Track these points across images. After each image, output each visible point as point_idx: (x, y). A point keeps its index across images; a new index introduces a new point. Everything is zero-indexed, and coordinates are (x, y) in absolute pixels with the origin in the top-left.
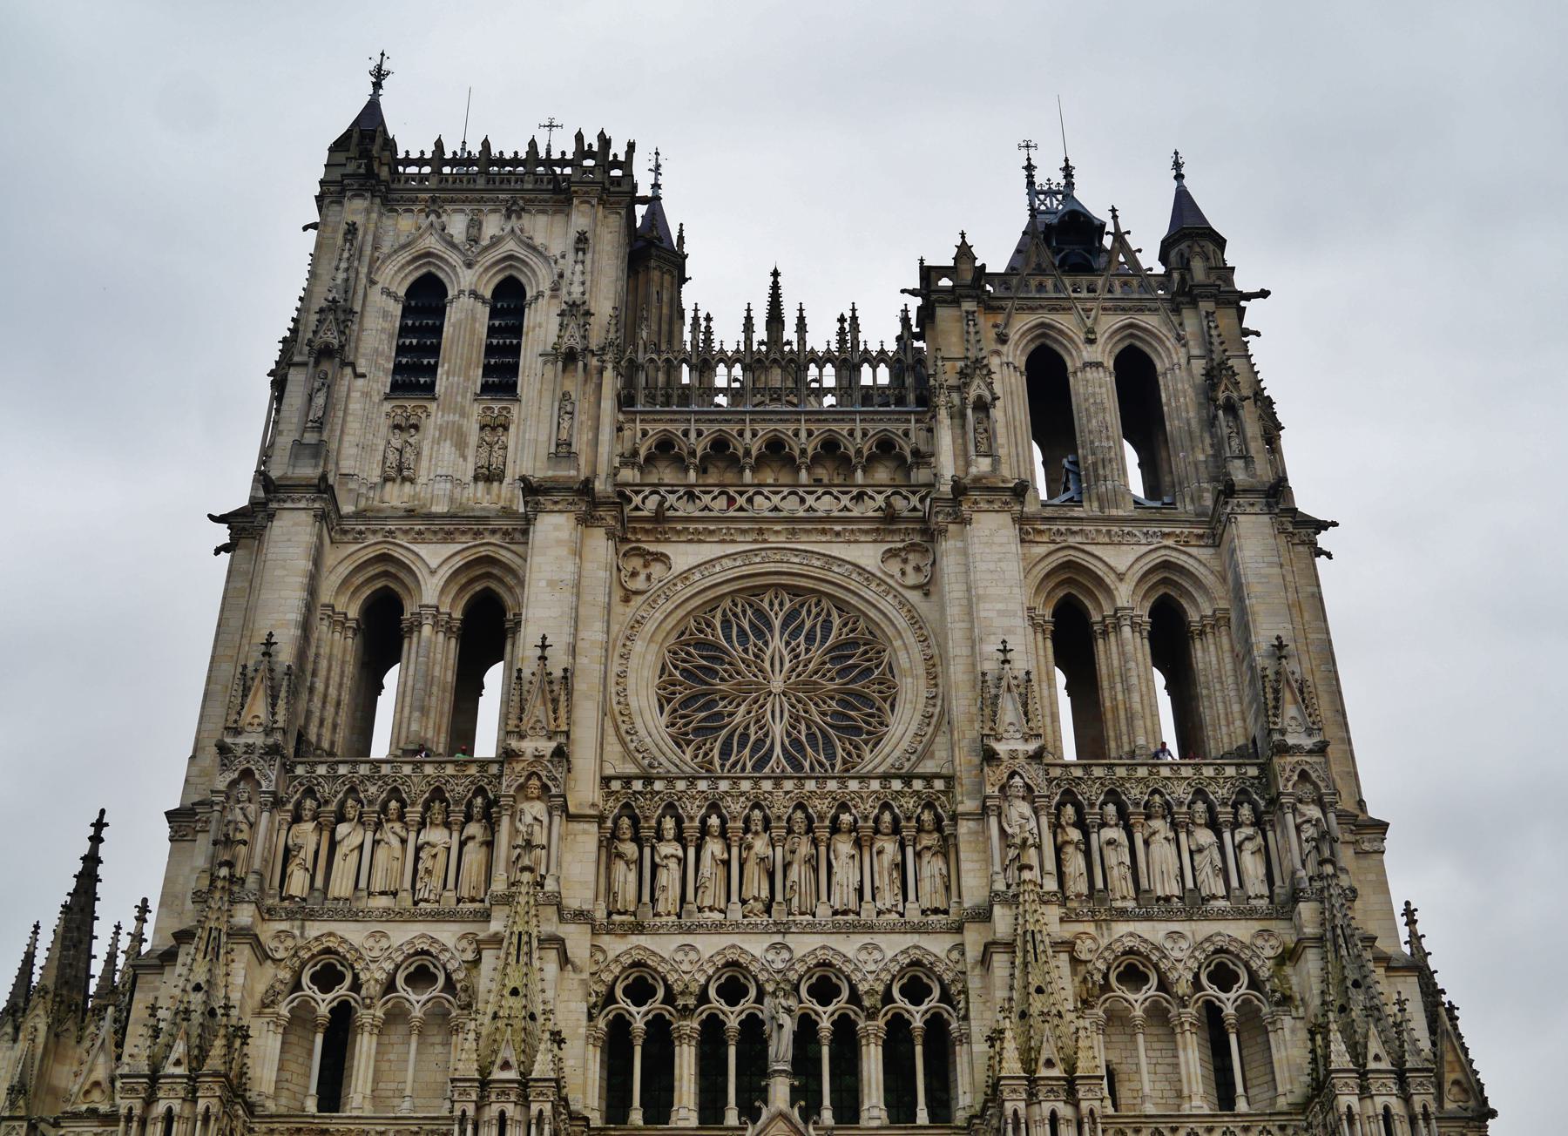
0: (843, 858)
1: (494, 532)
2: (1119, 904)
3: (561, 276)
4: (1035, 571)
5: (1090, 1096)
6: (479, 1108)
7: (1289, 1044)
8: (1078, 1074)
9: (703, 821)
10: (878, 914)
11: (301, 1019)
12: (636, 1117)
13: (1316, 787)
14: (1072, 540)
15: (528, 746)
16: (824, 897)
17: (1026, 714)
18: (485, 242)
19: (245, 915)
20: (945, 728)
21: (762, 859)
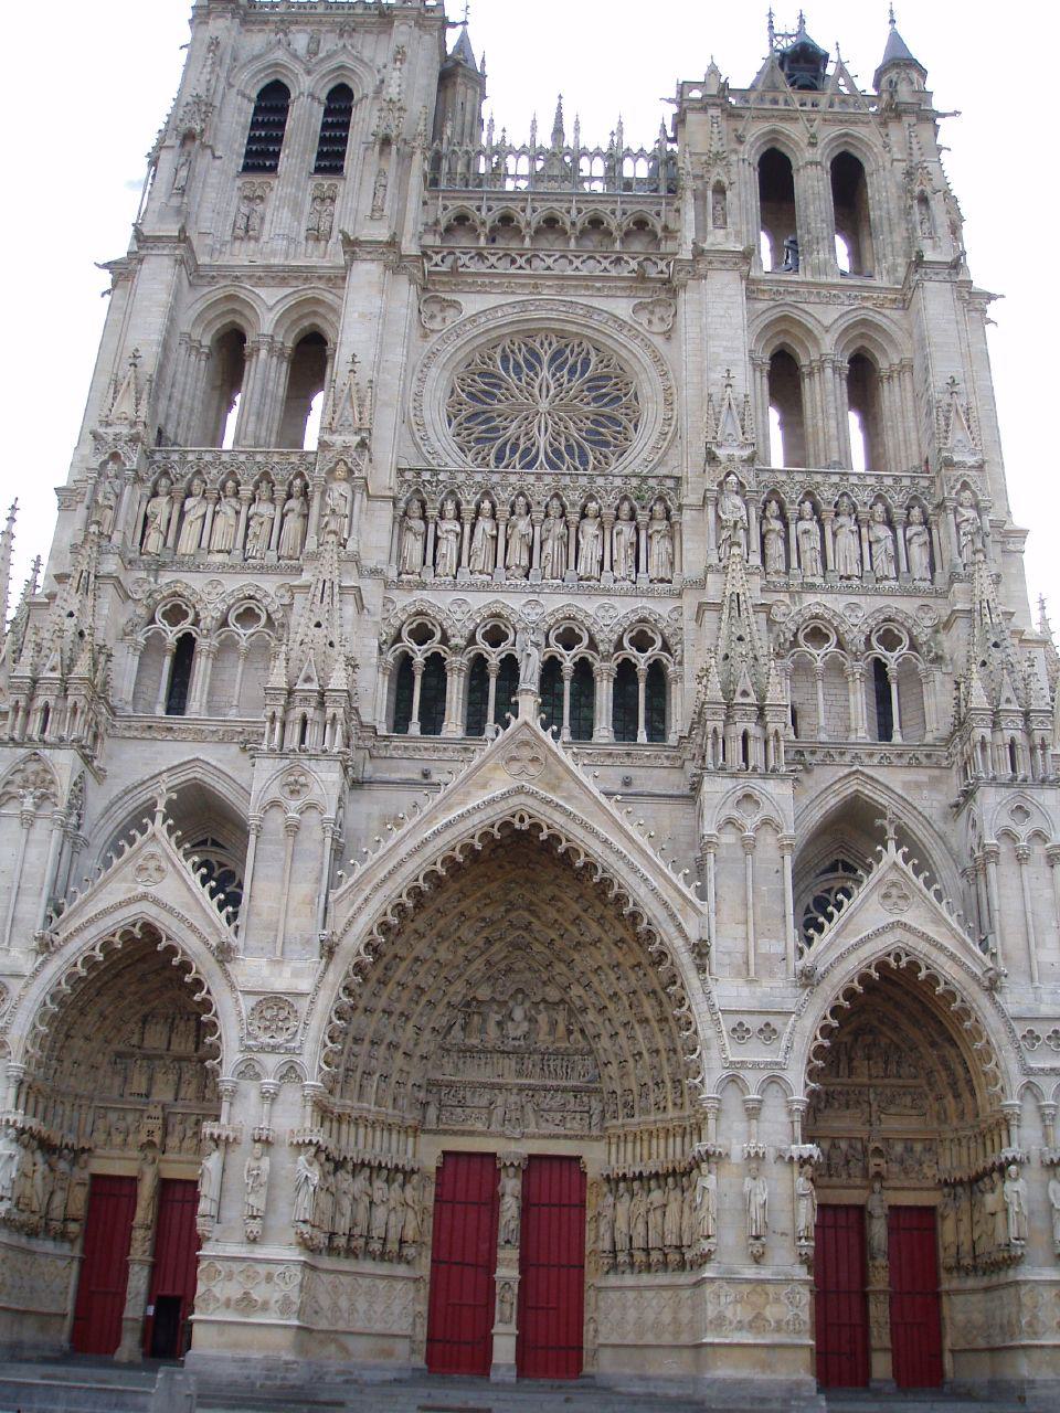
0: (589, 537)
1: (320, 278)
2: (809, 580)
3: (382, 81)
4: (757, 322)
6: (286, 711)
9: (478, 506)
10: (615, 581)
11: (153, 644)
12: (415, 728)
13: (973, 493)
14: (790, 299)
15: (338, 440)
16: (572, 566)
17: (743, 427)
18: (321, 55)
19: (111, 565)
20: (677, 443)
21: (523, 536)
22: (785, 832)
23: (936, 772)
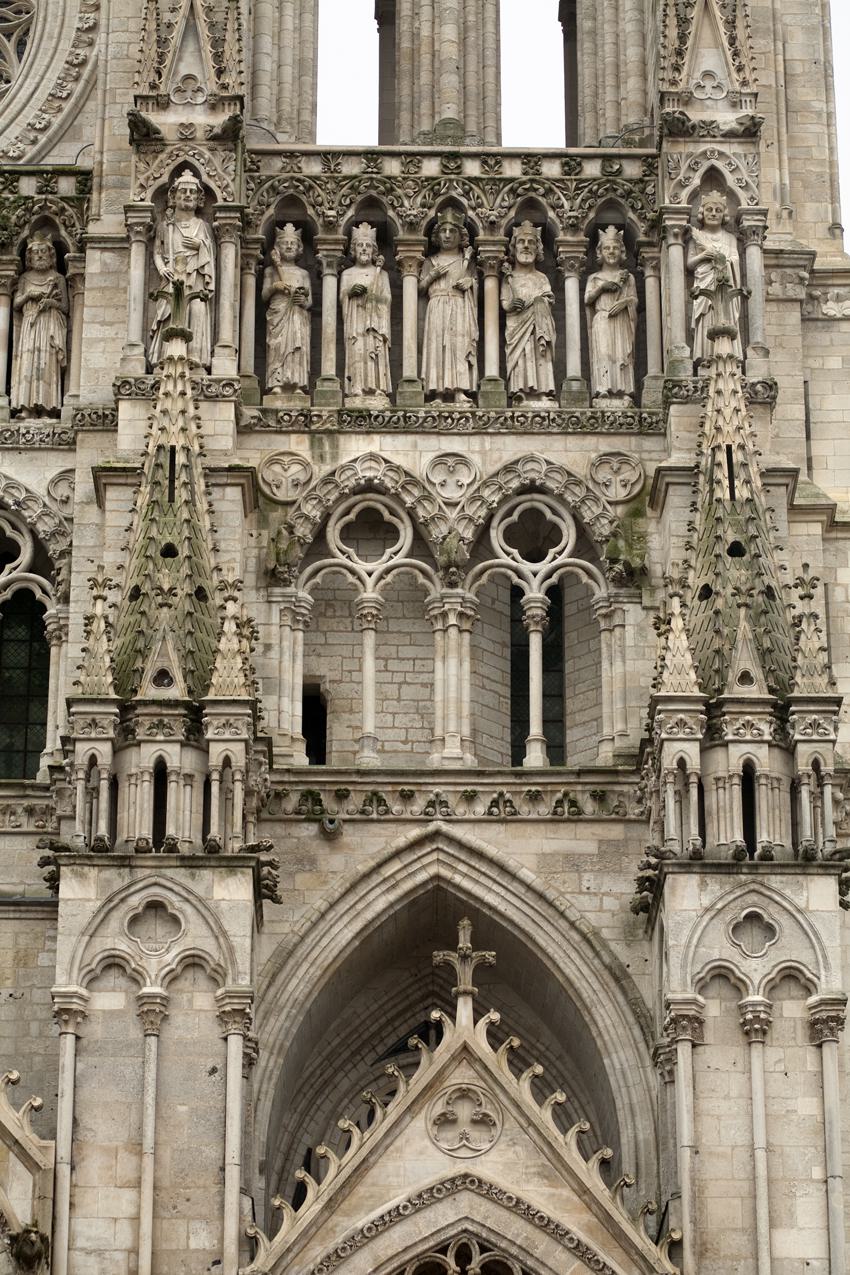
2: (357, 403)
5: (227, 736)
7: (630, 653)
8: (211, 696)
13: (732, 196)
22: (230, 985)
23: (616, 831)
